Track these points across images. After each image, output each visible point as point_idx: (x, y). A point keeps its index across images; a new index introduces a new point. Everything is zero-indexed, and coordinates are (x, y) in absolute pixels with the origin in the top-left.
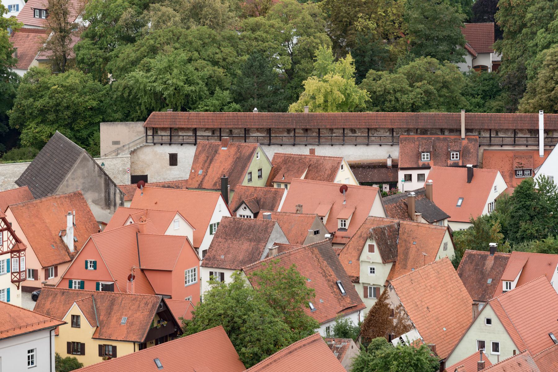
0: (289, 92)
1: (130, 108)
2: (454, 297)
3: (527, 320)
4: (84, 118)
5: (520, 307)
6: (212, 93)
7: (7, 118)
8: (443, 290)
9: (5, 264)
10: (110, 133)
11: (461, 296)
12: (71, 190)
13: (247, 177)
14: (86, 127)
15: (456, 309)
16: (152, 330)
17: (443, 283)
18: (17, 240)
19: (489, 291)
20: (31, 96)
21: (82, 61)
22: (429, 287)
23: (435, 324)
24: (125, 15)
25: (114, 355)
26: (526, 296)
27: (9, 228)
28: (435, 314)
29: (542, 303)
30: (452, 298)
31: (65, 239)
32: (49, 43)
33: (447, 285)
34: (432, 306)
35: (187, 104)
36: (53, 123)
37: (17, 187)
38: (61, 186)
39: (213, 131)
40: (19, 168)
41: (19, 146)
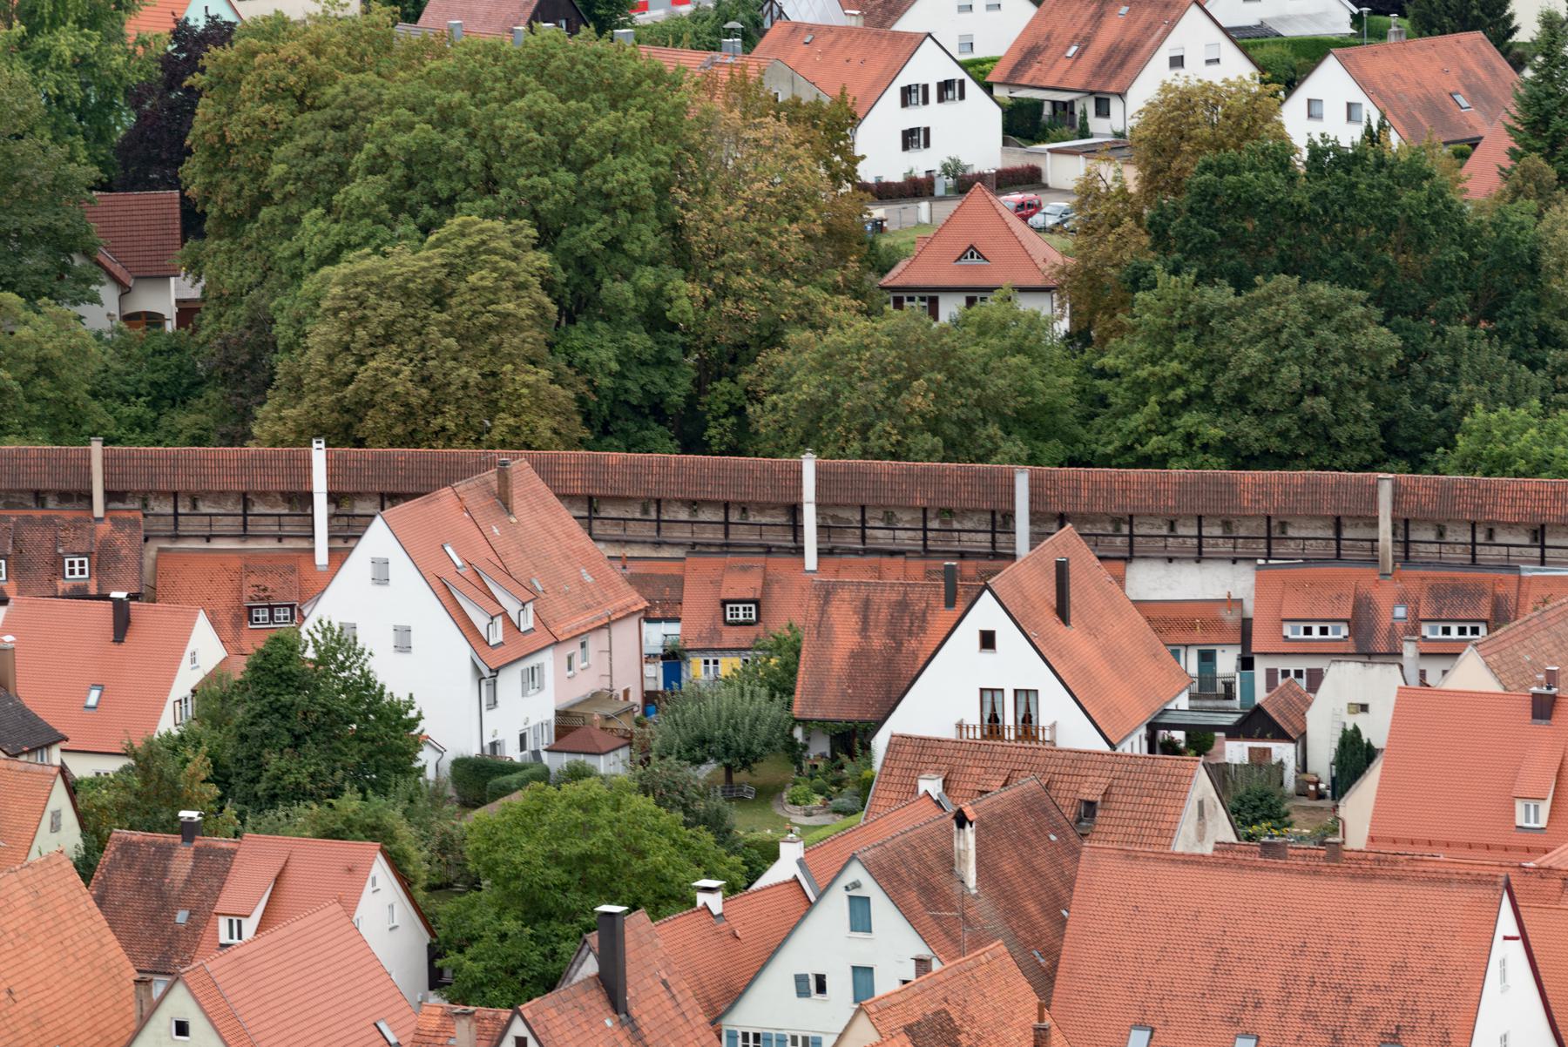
2: (83, 962)
3: (290, 1023)
5: (269, 989)
8: (52, 941)
11: (103, 959)
15: (90, 996)
17: (51, 924)
22: (12, 935)
23: (31, 1037)
26: (284, 957)
28: (31, 1009)
29: (331, 978)
30: (77, 965)
33: (62, 927)
34: (22, 986)
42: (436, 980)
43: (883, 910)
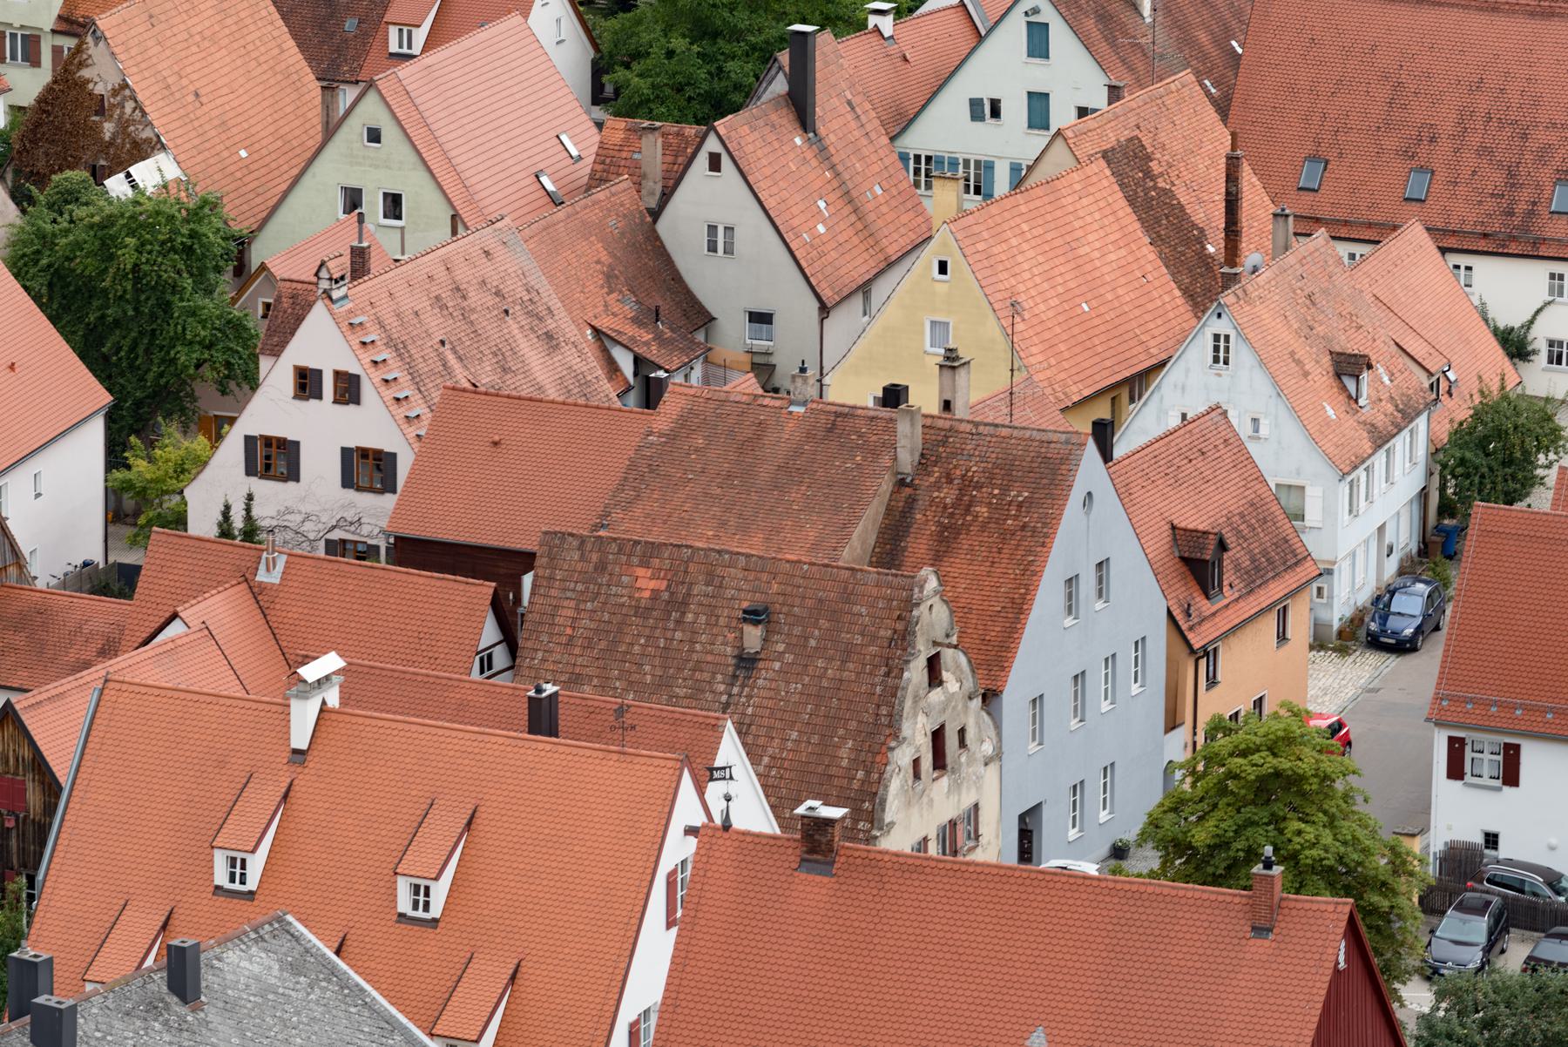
2: (265, 67)
3: (477, 133)
5: (457, 99)
8: (235, 45)
11: (283, 65)
15: (271, 101)
17: (234, 28)
19: (352, 52)
22: (198, 38)
23: (217, 140)
26: (471, 67)
28: (216, 112)
29: (515, 89)
30: (259, 70)
33: (245, 31)
34: (208, 89)
42: (598, 98)
43: (1061, 37)
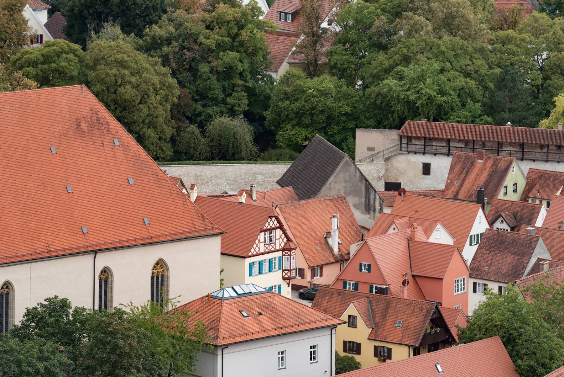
0: (538, 108)
1: (384, 115)
4: (338, 123)
6: (464, 105)
7: (264, 119)
9: (277, 261)
10: (365, 139)
12: (333, 193)
13: (503, 191)
14: (339, 132)
16: (426, 336)
18: (289, 239)
20: (287, 98)
21: (335, 66)
24: (377, 23)
25: (389, 357)
27: (281, 227)
31: (330, 240)
32: (299, 47)
35: (440, 114)
36: (307, 126)
37: (278, 187)
38: (324, 189)
39: (467, 143)
40: (281, 169)
41: (274, 147)
